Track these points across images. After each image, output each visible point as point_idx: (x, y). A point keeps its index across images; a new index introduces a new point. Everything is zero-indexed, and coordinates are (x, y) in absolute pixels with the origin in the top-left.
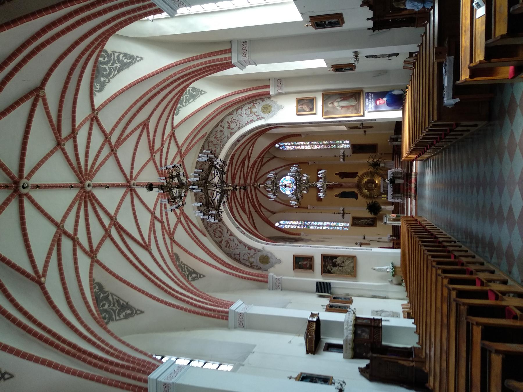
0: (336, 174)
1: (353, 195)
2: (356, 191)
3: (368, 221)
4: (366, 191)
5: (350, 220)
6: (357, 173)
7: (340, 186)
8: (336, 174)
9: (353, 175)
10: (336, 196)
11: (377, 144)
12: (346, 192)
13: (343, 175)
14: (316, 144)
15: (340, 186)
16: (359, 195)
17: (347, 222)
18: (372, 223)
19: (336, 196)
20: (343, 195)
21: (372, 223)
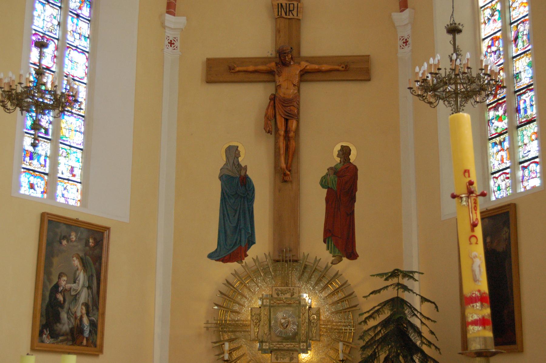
0: (345, 152)
1: (233, 241)
2: (260, 249)
3: (80, 310)
4: (253, 302)
5: (95, 215)
6: (352, 255)
7: (286, 172)
8: (345, 152)
9: (341, 234)
10: (232, 152)
11: (521, 350)
12: (251, 200)
13: (342, 187)
14: (508, 23)
15: (286, 172)
16: (234, 266)
17: (84, 200)
18: (65, 326)
19: (232, 152)
20: (237, 190)
21: (65, 326)
